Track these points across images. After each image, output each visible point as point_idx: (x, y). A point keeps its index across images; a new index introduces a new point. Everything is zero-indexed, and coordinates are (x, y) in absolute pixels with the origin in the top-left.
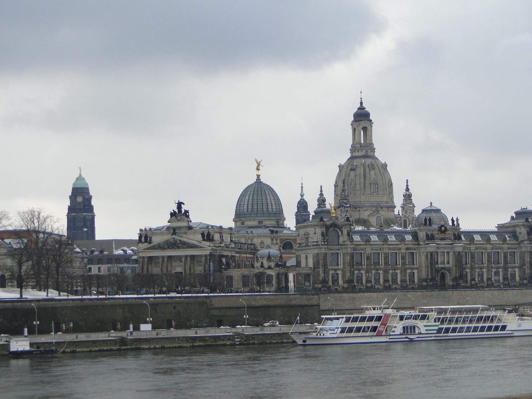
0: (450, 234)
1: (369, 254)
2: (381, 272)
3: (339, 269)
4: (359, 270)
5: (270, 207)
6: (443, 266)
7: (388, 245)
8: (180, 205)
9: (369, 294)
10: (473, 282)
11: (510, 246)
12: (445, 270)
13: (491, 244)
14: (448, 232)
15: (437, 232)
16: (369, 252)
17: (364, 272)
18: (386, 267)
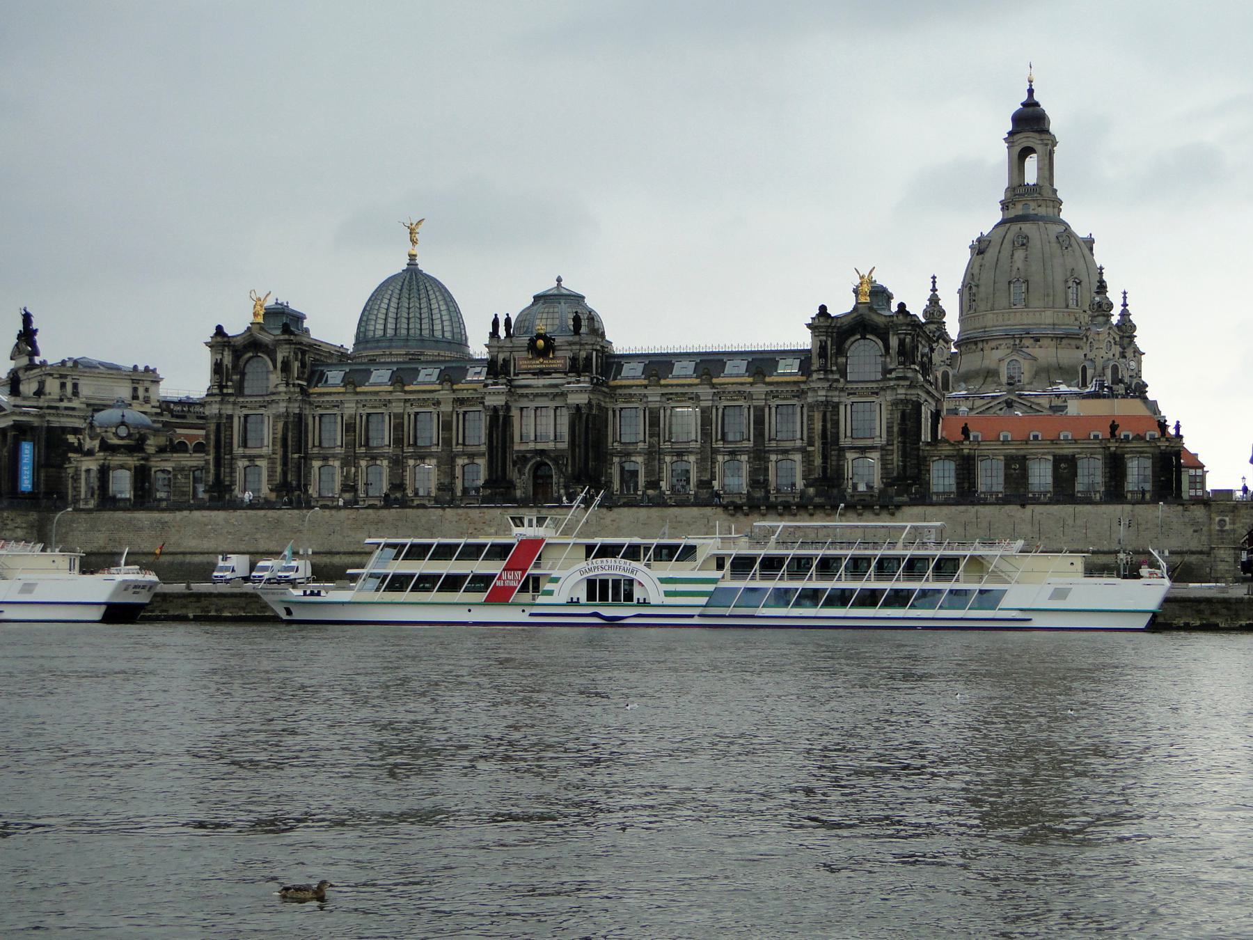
0: (560, 359)
1: (350, 417)
2: (385, 463)
3: (260, 456)
4: (325, 458)
5: (438, 327)
6: (540, 446)
7: (406, 392)
8: (27, 318)
9: (206, 513)
10: (650, 492)
11: (771, 388)
12: (549, 457)
13: (713, 386)
14: (558, 353)
15: (525, 354)
16: (352, 411)
17: (337, 464)
18: (398, 451)
